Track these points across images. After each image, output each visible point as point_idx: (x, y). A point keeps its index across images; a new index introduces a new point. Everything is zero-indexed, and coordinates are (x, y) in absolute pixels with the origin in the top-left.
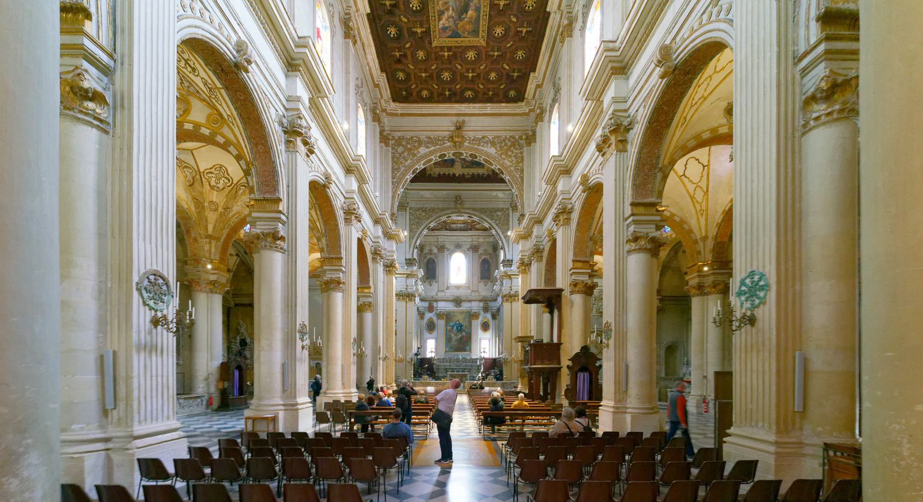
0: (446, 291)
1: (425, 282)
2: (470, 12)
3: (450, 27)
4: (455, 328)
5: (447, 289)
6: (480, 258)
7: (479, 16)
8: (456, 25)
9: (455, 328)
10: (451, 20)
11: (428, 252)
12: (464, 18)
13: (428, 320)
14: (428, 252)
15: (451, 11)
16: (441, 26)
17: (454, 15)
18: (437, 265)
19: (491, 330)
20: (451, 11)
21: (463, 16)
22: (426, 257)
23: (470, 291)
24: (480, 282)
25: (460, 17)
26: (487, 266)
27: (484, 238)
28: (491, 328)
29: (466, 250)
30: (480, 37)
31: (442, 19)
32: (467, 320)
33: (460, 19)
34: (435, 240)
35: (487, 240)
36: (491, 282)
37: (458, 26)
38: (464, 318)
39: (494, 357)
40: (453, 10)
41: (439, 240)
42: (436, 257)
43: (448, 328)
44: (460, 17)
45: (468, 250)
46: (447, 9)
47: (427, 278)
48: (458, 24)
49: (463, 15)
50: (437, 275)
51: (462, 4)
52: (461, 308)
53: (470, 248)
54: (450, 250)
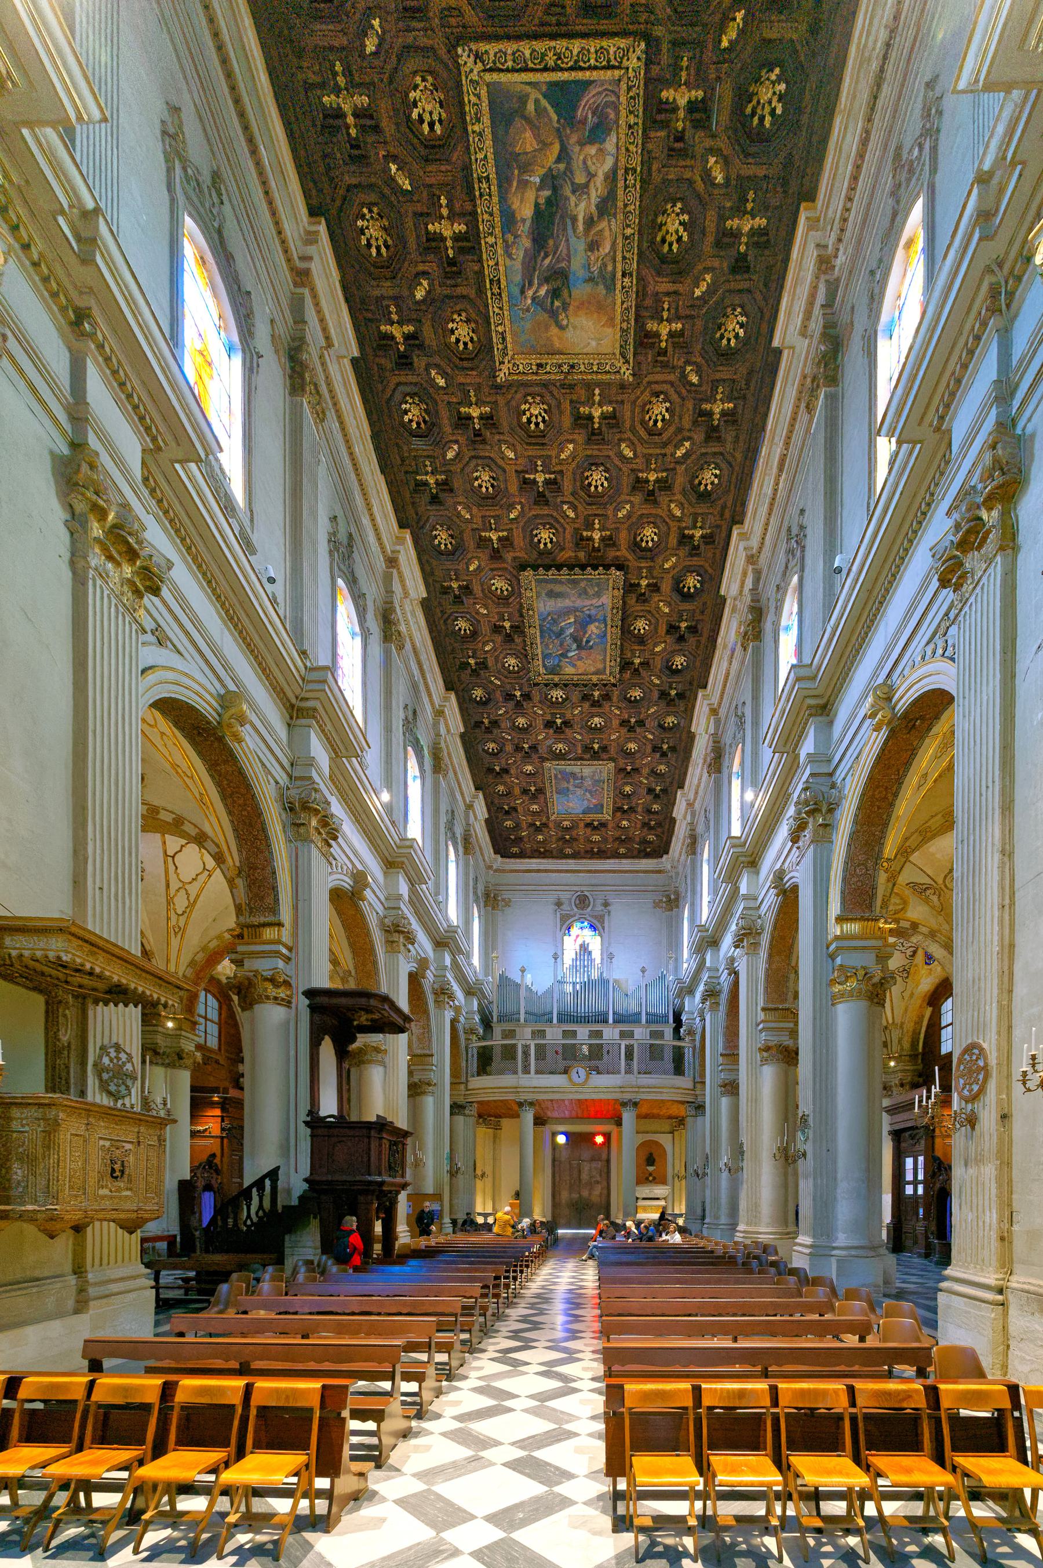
2: (526, 211)
3: (582, 144)
7: (503, 199)
8: (564, 155)
10: (580, 179)
12: (540, 188)
15: (581, 218)
16: (610, 145)
17: (573, 199)
20: (581, 218)
21: (547, 193)
25: (555, 189)
30: (484, 93)
31: (606, 177)
33: (551, 180)
37: (556, 148)
40: (574, 219)
44: (555, 189)
46: (590, 222)
48: (559, 160)
49: (549, 201)
51: (551, 242)
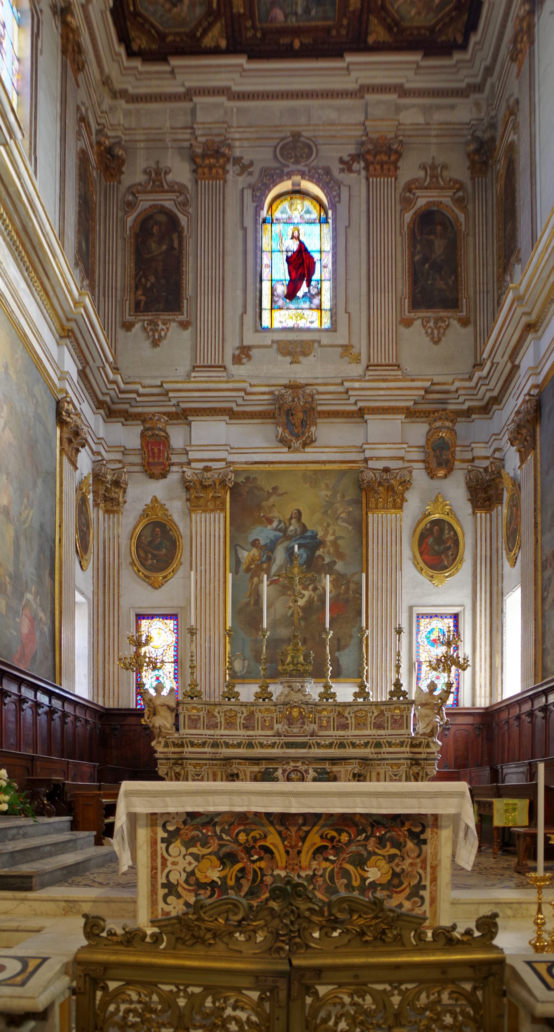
0: (234, 369)
1: (128, 326)
4: (280, 555)
5: (237, 360)
6: (407, 203)
9: (280, 555)
11: (141, 178)
13: (145, 514)
14: (141, 178)
18: (189, 246)
19: (466, 568)
22: (131, 206)
23: (357, 370)
24: (408, 323)
26: (439, 245)
27: (426, 110)
28: (467, 553)
29: (335, 168)
32: (342, 510)
34: (182, 121)
35: (438, 117)
36: (465, 322)
38: (330, 504)
39: (483, 702)
41: (200, 117)
42: (185, 204)
43: (244, 555)
45: (347, 166)
47: (138, 308)
50: (189, 289)
52: (310, 454)
53: (355, 157)
54: (256, 169)
